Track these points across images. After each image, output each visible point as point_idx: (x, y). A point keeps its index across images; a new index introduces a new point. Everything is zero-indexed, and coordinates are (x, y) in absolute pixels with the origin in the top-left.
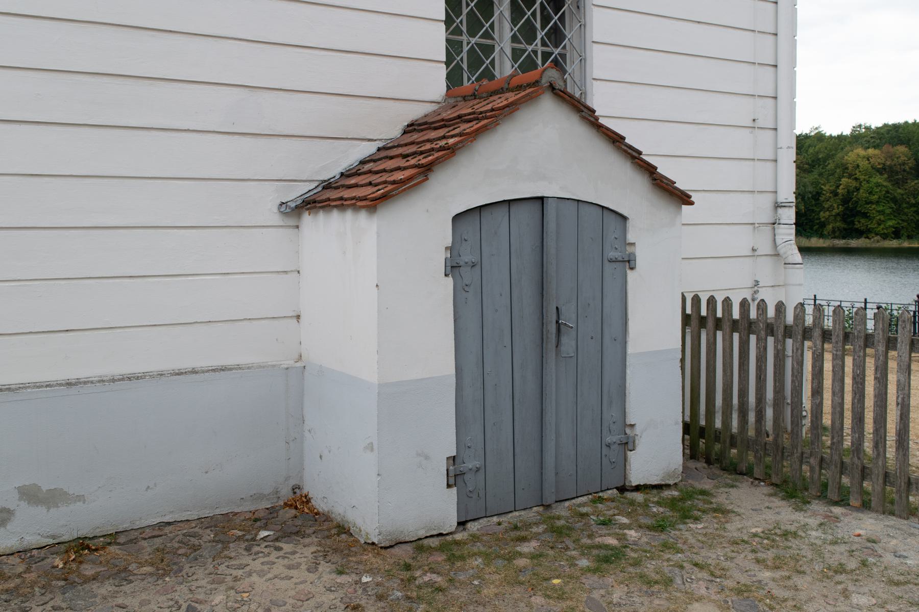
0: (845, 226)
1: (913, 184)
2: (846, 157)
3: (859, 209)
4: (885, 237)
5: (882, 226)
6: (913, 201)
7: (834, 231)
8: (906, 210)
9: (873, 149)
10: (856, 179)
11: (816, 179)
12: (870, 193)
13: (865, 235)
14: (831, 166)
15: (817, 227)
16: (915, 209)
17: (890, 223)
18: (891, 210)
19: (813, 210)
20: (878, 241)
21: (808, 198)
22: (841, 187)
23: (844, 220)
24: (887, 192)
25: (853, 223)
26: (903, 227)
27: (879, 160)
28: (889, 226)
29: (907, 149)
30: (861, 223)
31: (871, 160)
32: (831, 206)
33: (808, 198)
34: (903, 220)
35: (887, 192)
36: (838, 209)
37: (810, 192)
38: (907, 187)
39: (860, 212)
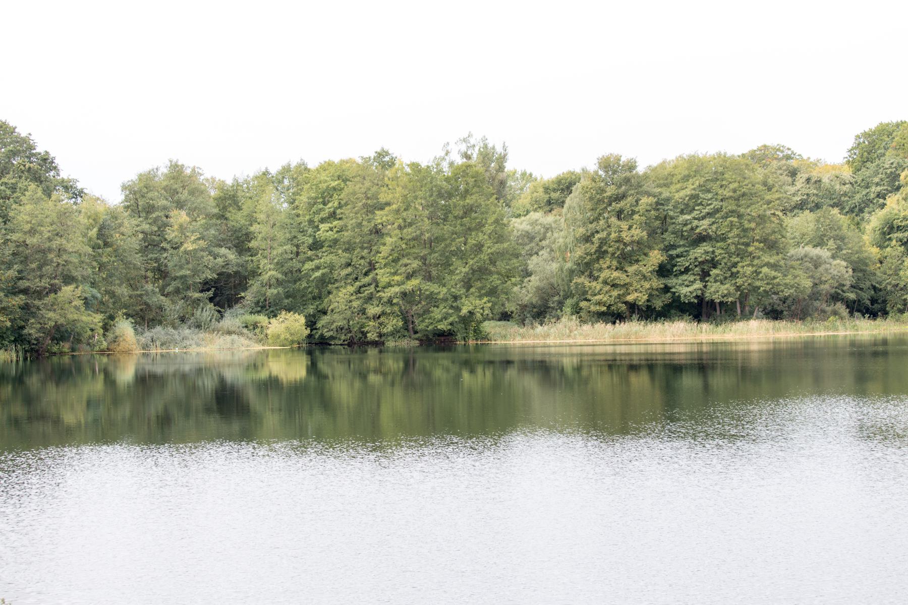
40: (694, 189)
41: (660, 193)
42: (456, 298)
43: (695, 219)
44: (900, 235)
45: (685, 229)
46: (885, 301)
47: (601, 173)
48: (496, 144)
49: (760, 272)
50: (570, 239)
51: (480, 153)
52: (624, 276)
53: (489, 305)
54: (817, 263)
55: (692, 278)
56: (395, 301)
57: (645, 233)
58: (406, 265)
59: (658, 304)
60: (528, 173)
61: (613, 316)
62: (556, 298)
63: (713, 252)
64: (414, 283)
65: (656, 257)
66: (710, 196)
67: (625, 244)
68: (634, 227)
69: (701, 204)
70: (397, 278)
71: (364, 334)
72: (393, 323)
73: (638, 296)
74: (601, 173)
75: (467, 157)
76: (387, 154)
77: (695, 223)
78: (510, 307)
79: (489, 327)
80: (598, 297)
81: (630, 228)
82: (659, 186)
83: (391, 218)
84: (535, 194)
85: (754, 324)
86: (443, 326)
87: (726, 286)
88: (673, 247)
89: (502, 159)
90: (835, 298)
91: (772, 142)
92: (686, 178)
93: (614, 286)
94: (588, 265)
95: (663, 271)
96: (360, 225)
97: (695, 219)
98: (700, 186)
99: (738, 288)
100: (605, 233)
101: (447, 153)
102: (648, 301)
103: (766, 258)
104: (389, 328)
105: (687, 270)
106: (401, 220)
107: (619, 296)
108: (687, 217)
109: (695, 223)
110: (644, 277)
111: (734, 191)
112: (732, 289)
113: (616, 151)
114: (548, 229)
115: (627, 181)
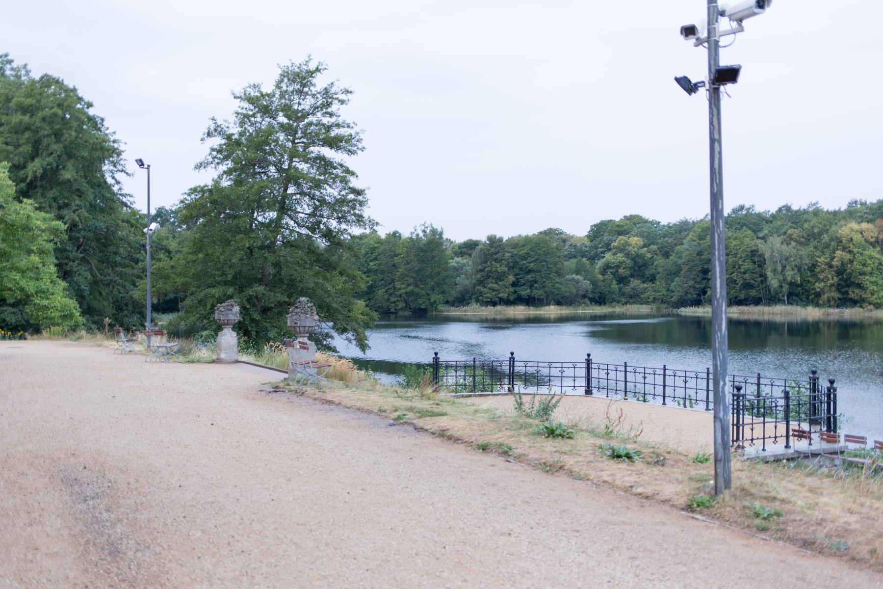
0: (840, 296)
2: (840, 231)
3: (852, 280)
5: (875, 296)
7: (829, 301)
10: (850, 252)
11: (811, 251)
13: (859, 305)
14: (826, 238)
15: (813, 296)
19: (809, 281)
20: (871, 311)
21: (805, 270)
22: (836, 259)
23: (839, 290)
25: (847, 293)
27: (872, 234)
30: (854, 293)
32: (826, 277)
33: (805, 270)
36: (833, 279)
37: (806, 264)
39: (854, 283)
42: (428, 295)
44: (611, 270)
46: (605, 298)
47: (488, 242)
51: (431, 231)
54: (577, 282)
59: (512, 298)
64: (410, 288)
65: (511, 278)
71: (389, 309)
72: (401, 305)
73: (504, 295)
74: (488, 242)
76: (398, 232)
77: (528, 265)
78: (450, 299)
79: (440, 307)
81: (501, 266)
82: (512, 248)
83: (401, 261)
85: (552, 307)
86: (423, 307)
88: (518, 274)
89: (441, 234)
90: (584, 296)
91: (554, 226)
92: (524, 246)
93: (494, 290)
94: (482, 281)
95: (514, 284)
96: (387, 263)
99: (545, 292)
103: (558, 280)
104: (400, 307)
105: (524, 284)
108: (524, 262)
109: (528, 265)
110: (506, 287)
112: (543, 293)
113: (494, 233)
114: (464, 265)
115: (500, 245)
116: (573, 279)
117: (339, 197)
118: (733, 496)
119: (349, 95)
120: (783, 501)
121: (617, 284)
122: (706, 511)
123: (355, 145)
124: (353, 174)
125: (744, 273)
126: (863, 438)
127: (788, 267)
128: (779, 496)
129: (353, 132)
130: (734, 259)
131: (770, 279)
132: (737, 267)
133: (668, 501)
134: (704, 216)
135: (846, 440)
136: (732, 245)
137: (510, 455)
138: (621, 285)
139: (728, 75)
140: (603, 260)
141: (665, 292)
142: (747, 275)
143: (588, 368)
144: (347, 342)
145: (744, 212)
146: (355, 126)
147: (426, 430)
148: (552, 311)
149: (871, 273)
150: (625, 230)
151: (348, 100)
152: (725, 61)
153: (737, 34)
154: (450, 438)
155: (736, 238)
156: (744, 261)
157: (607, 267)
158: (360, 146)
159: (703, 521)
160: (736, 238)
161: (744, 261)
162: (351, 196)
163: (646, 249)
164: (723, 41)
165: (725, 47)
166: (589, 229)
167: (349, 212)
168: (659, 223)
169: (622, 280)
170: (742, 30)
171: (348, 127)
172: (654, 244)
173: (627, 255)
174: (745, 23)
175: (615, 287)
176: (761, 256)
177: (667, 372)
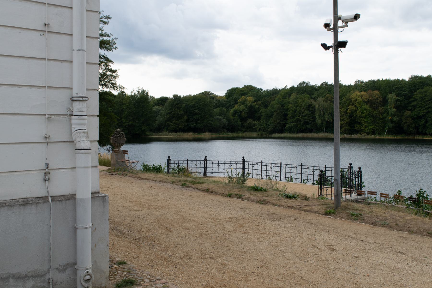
1: (381, 109)
2: (351, 96)
3: (357, 120)
4: (368, 133)
5: (367, 129)
6: (381, 117)
7: (345, 131)
8: (378, 121)
9: (363, 92)
10: (356, 106)
12: (362, 113)
13: (359, 133)
16: (382, 121)
17: (371, 127)
18: (371, 121)
20: (365, 136)
22: (349, 110)
24: (370, 112)
25: (354, 127)
26: (376, 129)
27: (366, 97)
28: (370, 128)
29: (379, 92)
30: (357, 127)
31: (362, 97)
34: (376, 126)
35: (370, 112)
36: (347, 120)
38: (378, 110)
40: (194, 103)
41: (187, 103)
43: (194, 109)
45: (192, 112)
47: (173, 98)
48: (146, 89)
49: (209, 122)
50: (166, 113)
51: (142, 91)
52: (178, 122)
53: (149, 128)
54: (220, 120)
55: (193, 123)
56: (127, 126)
57: (183, 112)
58: (129, 118)
60: (152, 96)
61: (176, 131)
62: (162, 127)
63: (198, 117)
65: (186, 118)
66: (198, 104)
67: (179, 115)
68: (181, 111)
69: (196, 106)
70: (127, 121)
74: (173, 98)
75: (138, 92)
79: (148, 133)
80: (173, 127)
81: (180, 111)
82: (186, 102)
84: (154, 102)
85: (207, 133)
87: (201, 125)
89: (147, 93)
90: (223, 128)
92: (192, 100)
93: (176, 124)
95: (187, 121)
97: (194, 109)
98: (196, 102)
100: (174, 112)
101: (133, 91)
102: (184, 128)
106: (128, 108)
107: (177, 127)
109: (195, 110)
111: (203, 103)
113: (177, 94)
114: (160, 110)
115: (179, 100)
116: (218, 118)
117: (102, 73)
118: (342, 209)
119: (109, 20)
120: (360, 210)
121: (241, 121)
122: (333, 215)
123: (111, 46)
124: (111, 61)
125: (305, 116)
126: (375, 192)
127: (326, 114)
128: (358, 209)
129: (110, 39)
130: (300, 109)
131: (317, 119)
132: (301, 113)
133: (317, 212)
134: (285, 87)
135: (368, 194)
136: (299, 102)
137: (243, 198)
138: (243, 122)
139: (343, 44)
140: (234, 109)
141: (265, 126)
142: (306, 117)
143: (243, 164)
144: (107, 152)
145: (305, 85)
146: (111, 36)
147: (199, 189)
148: (207, 135)
149: (365, 117)
150: (245, 93)
151: (108, 22)
152: (341, 38)
153: (345, 28)
154: (212, 192)
155: (301, 98)
156: (305, 110)
157: (235, 112)
158: (114, 46)
159: (333, 218)
160: (301, 98)
161: (305, 110)
162: (109, 73)
163: (255, 103)
164: (340, 30)
165: (340, 32)
166: (226, 92)
167: (108, 82)
168: (262, 90)
169: (244, 119)
170: (347, 26)
171: (108, 36)
172: (259, 100)
173: (246, 106)
174: (349, 24)
175: (239, 123)
176: (314, 107)
177: (282, 165)
